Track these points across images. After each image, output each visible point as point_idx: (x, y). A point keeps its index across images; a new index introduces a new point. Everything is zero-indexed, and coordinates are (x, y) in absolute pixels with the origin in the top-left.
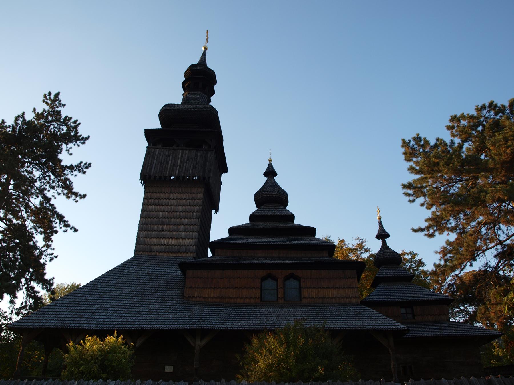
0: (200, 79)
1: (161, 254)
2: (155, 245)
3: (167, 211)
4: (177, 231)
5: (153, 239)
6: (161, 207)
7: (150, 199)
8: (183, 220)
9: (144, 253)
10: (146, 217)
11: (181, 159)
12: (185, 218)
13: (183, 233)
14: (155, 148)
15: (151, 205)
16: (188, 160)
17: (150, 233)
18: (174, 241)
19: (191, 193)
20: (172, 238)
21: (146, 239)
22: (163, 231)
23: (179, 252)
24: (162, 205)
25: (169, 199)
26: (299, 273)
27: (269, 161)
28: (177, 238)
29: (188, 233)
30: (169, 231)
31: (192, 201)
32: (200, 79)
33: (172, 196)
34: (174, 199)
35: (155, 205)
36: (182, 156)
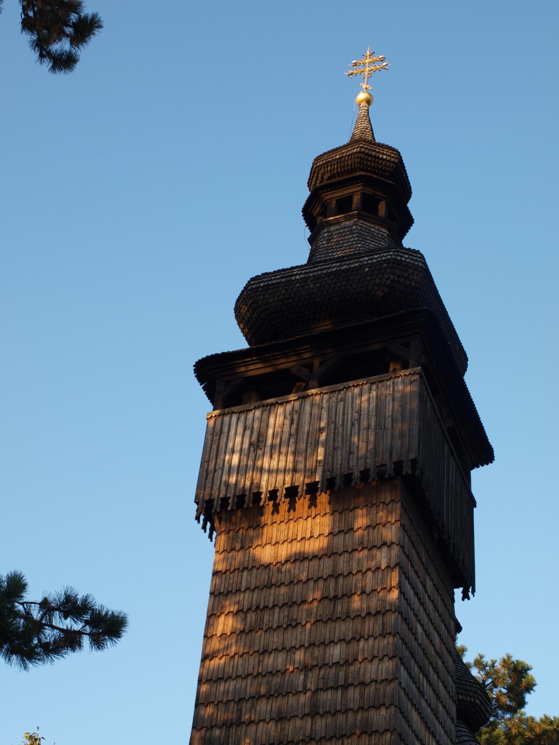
14: (429, 395)
33: (429, 584)
34: (429, 597)
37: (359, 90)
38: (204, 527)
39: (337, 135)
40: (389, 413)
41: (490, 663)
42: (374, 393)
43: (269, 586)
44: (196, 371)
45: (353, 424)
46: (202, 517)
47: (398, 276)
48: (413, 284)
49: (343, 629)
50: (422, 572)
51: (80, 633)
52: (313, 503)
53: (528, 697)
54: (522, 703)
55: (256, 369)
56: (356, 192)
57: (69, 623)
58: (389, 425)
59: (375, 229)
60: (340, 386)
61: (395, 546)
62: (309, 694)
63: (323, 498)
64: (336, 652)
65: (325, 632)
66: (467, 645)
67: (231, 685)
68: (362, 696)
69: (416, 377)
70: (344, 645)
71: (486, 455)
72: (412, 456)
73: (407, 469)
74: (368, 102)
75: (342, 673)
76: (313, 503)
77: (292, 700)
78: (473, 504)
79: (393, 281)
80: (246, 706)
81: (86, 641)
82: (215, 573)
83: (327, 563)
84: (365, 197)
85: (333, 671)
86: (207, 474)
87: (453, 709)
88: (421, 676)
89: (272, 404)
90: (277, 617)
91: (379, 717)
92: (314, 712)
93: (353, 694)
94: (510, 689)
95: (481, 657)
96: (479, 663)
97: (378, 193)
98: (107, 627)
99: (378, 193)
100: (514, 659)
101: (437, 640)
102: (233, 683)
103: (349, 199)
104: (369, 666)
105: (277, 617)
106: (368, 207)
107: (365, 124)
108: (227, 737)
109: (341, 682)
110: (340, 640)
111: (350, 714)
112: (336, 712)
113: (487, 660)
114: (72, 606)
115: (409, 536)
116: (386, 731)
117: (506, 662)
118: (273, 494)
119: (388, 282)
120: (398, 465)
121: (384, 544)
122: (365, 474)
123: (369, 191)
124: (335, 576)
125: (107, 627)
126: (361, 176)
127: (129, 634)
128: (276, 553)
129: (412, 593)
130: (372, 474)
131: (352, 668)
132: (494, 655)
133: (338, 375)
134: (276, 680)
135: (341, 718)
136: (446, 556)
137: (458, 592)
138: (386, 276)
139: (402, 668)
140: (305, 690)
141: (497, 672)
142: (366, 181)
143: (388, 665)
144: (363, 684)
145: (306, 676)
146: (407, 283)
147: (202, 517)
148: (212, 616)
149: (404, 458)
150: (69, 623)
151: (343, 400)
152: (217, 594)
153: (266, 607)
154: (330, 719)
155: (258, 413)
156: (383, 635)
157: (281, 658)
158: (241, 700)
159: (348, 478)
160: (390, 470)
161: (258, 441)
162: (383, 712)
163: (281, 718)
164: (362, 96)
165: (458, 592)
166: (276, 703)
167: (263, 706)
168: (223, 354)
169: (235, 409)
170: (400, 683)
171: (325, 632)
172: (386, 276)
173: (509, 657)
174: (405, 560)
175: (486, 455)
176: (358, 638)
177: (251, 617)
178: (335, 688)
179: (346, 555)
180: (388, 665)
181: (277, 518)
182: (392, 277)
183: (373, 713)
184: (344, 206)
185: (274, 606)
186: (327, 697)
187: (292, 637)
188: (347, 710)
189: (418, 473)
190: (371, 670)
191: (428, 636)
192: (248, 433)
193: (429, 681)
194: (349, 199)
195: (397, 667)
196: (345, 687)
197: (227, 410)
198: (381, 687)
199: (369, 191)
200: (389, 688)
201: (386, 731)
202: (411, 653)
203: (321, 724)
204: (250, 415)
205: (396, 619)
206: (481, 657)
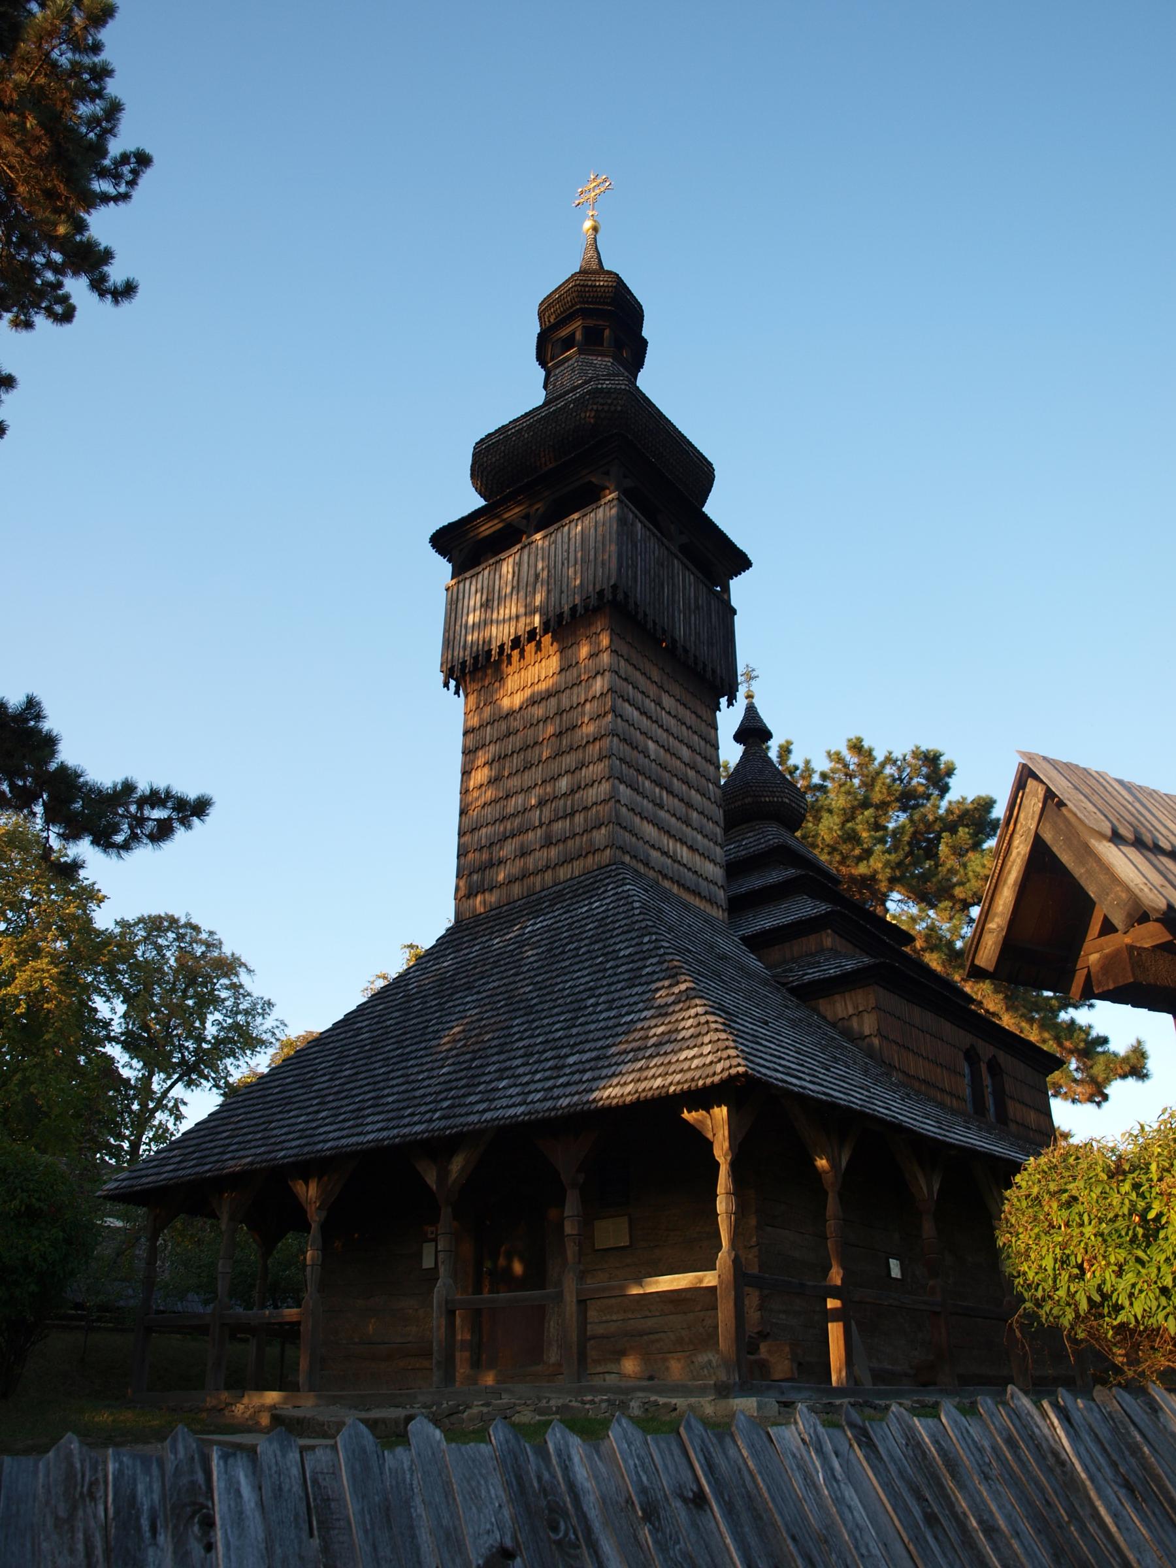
0: (595, 322)
1: (667, 884)
2: (653, 846)
3: (663, 747)
4: (687, 823)
5: (645, 823)
6: (649, 722)
7: (626, 680)
8: (693, 792)
9: (634, 863)
10: (625, 740)
11: (684, 595)
12: (698, 791)
13: (699, 837)
14: (637, 517)
15: (628, 701)
16: (697, 607)
17: (639, 799)
18: (684, 853)
19: (698, 716)
20: (683, 842)
21: (631, 814)
22: (661, 807)
23: (696, 893)
24: (650, 718)
25: (659, 704)
26: (1005, 1059)
27: (747, 697)
28: (691, 848)
29: (706, 841)
30: (674, 815)
31: (702, 743)
32: (595, 322)
33: (667, 701)
34: (669, 713)
35: (638, 709)
36: (684, 587)
37: (586, 217)
38: (457, 693)
39: (557, 270)
40: (592, 544)
41: (901, 757)
42: (579, 528)
43: (508, 735)
44: (434, 546)
45: (563, 564)
46: (452, 683)
47: (602, 405)
48: (619, 408)
49: (569, 761)
50: (652, 690)
51: (170, 819)
52: (539, 648)
53: (952, 782)
54: (945, 789)
55: (487, 529)
56: (576, 327)
57: (158, 814)
58: (592, 557)
59: (597, 360)
60: (551, 529)
61: (607, 673)
62: (544, 827)
63: (547, 639)
64: (564, 784)
65: (554, 767)
66: (873, 745)
68: (586, 820)
69: (615, 502)
70: (570, 776)
71: (741, 562)
72: (612, 582)
73: (608, 596)
74: (595, 229)
75: (569, 803)
76: (539, 648)
77: (531, 835)
78: (734, 612)
79: (597, 410)
80: (496, 848)
81: (176, 824)
82: (465, 733)
83: (553, 701)
84: (587, 331)
85: (562, 801)
87: (719, 814)
88: (657, 790)
89: (497, 562)
90: (517, 761)
91: (600, 836)
92: (548, 843)
93: (579, 819)
94: (927, 778)
95: (890, 753)
96: (889, 760)
97: (601, 323)
98: (194, 809)
99: (601, 323)
100: (923, 748)
101: (685, 752)
102: (484, 830)
103: (573, 334)
104: (590, 790)
105: (517, 761)
106: (592, 341)
107: (591, 253)
108: (483, 880)
109: (569, 811)
110: (566, 772)
111: (577, 838)
112: (566, 838)
113: (898, 754)
114: (155, 798)
115: (627, 660)
116: (606, 847)
117: (916, 754)
118: (502, 647)
119: (593, 414)
120: (601, 593)
121: (598, 673)
122: (574, 609)
123: (591, 323)
124: (560, 713)
125: (194, 809)
126: (581, 309)
127: (214, 812)
128: (512, 703)
129: (636, 713)
130: (580, 610)
131: (577, 796)
132: (902, 749)
133: (551, 518)
134: (517, 821)
135: (570, 843)
136: (709, 670)
137: (724, 701)
138: (590, 407)
139: (622, 787)
140: (541, 825)
141: (910, 765)
142: (584, 313)
143: (605, 787)
144: (586, 808)
145: (541, 811)
146: (613, 408)
147: (452, 683)
148: (466, 773)
149: (605, 586)
150: (158, 814)
151: (555, 542)
152: (468, 752)
153: (506, 756)
154: (561, 846)
156: (600, 759)
157: (520, 799)
158: (491, 844)
160: (593, 602)
161: (487, 600)
162: (603, 830)
163: (524, 853)
164: (588, 224)
165: (724, 701)
166: (517, 841)
168: (450, 524)
169: (467, 575)
170: (619, 801)
171: (554, 767)
172: (590, 407)
173: (918, 748)
174: (619, 682)
175: (741, 562)
176: (582, 765)
177: (496, 765)
179: (568, 691)
180: (605, 787)
181: (510, 670)
182: (595, 407)
183: (595, 833)
184: (568, 343)
185: (513, 752)
186: (558, 826)
187: (528, 778)
188: (575, 835)
189: (620, 597)
190: (592, 794)
191: (667, 750)
192: (479, 595)
193: (670, 792)
194: (573, 334)
195: (613, 786)
196: (572, 814)
197: (460, 578)
198: (600, 808)
199: (591, 323)
200: (607, 808)
201: (606, 847)
202: (638, 770)
203: (553, 852)
204: (480, 577)
205: (612, 741)
206: (890, 753)
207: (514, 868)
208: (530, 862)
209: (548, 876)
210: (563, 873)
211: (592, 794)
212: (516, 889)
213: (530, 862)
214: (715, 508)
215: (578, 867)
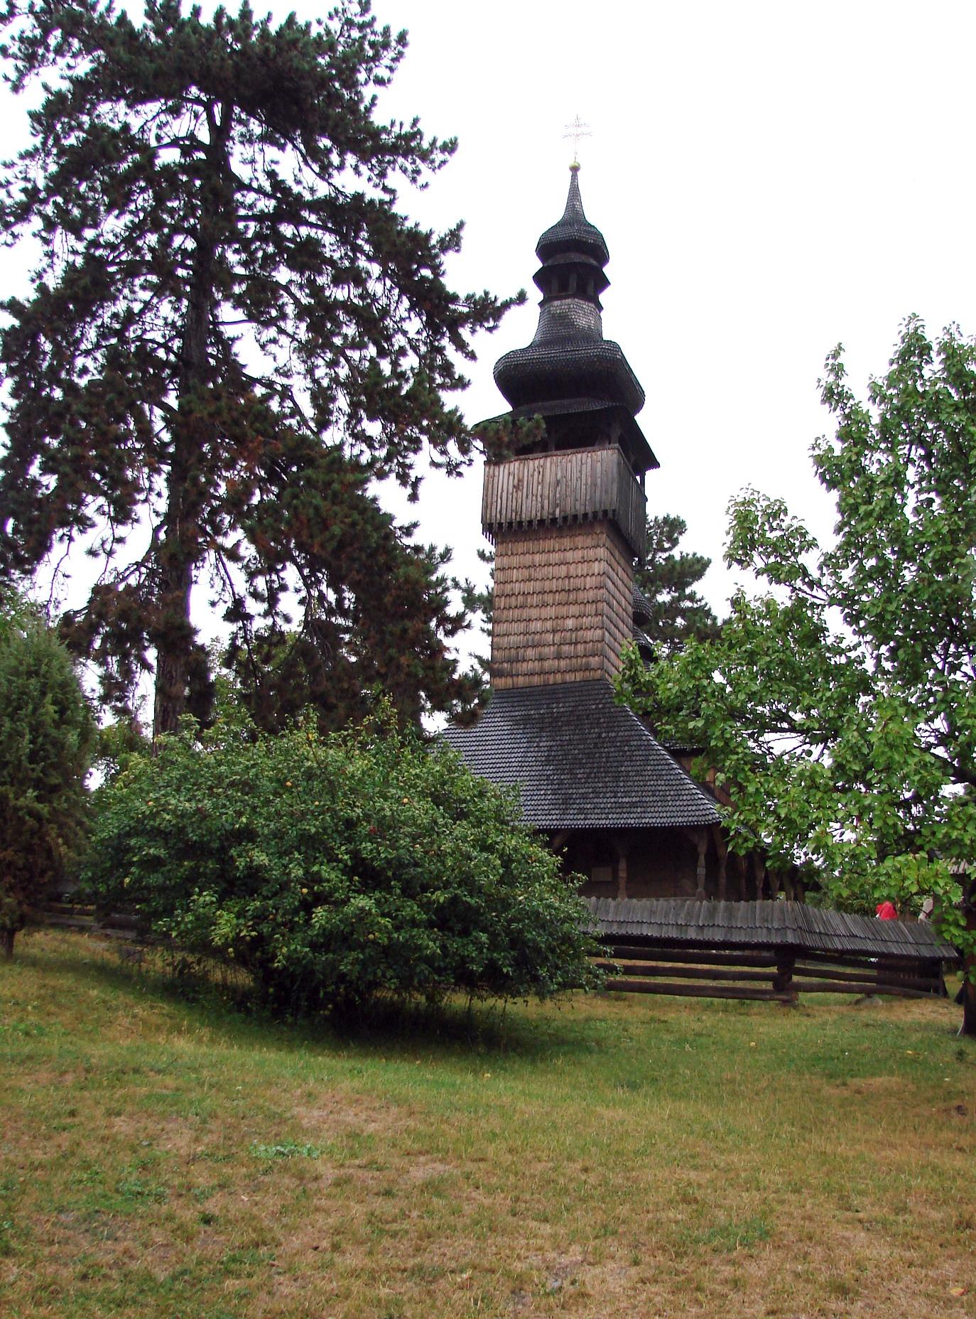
43: (530, 580)
54: (675, 543)
64: (570, 623)
67: (512, 638)
71: (657, 465)
73: (610, 515)
77: (546, 650)
83: (564, 568)
86: (486, 507)
91: (594, 661)
92: (559, 657)
124: (568, 577)
134: (537, 637)
135: (574, 660)
143: (599, 632)
155: (517, 464)
156: (596, 615)
159: (575, 517)
163: (541, 659)
167: (530, 653)
175: (657, 465)
178: (570, 644)
186: (565, 648)
190: (589, 635)
196: (576, 644)
203: (563, 663)
207: (536, 666)
208: (547, 664)
209: (559, 677)
210: (569, 677)
211: (589, 635)
212: (536, 680)
213: (547, 664)
214: (642, 419)
215: (579, 676)
